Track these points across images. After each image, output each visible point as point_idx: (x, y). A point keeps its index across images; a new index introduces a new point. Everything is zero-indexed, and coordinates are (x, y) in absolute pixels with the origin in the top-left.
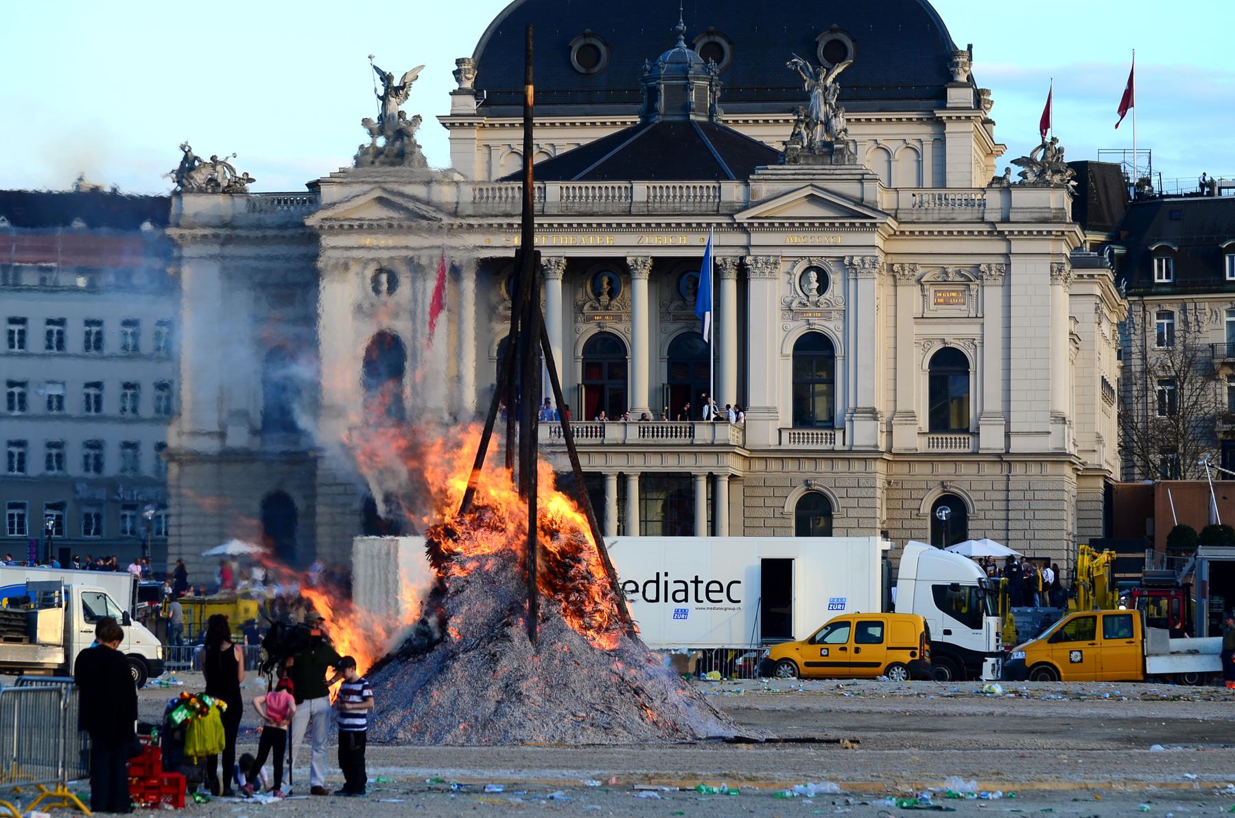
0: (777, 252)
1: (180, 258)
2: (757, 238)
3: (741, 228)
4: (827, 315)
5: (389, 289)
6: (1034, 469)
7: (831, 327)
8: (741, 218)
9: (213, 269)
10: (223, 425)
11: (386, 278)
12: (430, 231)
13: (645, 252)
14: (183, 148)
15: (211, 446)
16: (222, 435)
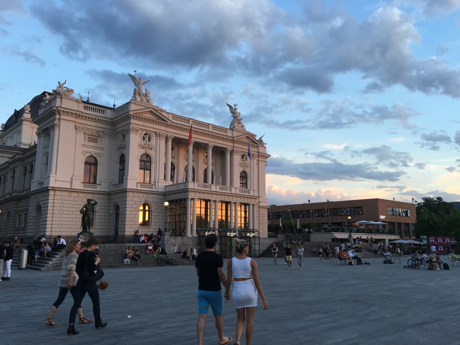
0: (239, 149)
1: (59, 119)
2: (235, 145)
3: (233, 141)
4: (247, 167)
5: (149, 141)
6: (263, 210)
7: (247, 170)
8: (235, 139)
9: (72, 125)
10: (72, 179)
11: (147, 136)
12: (164, 125)
13: (212, 143)
14: (59, 83)
15: (68, 186)
16: (72, 183)
